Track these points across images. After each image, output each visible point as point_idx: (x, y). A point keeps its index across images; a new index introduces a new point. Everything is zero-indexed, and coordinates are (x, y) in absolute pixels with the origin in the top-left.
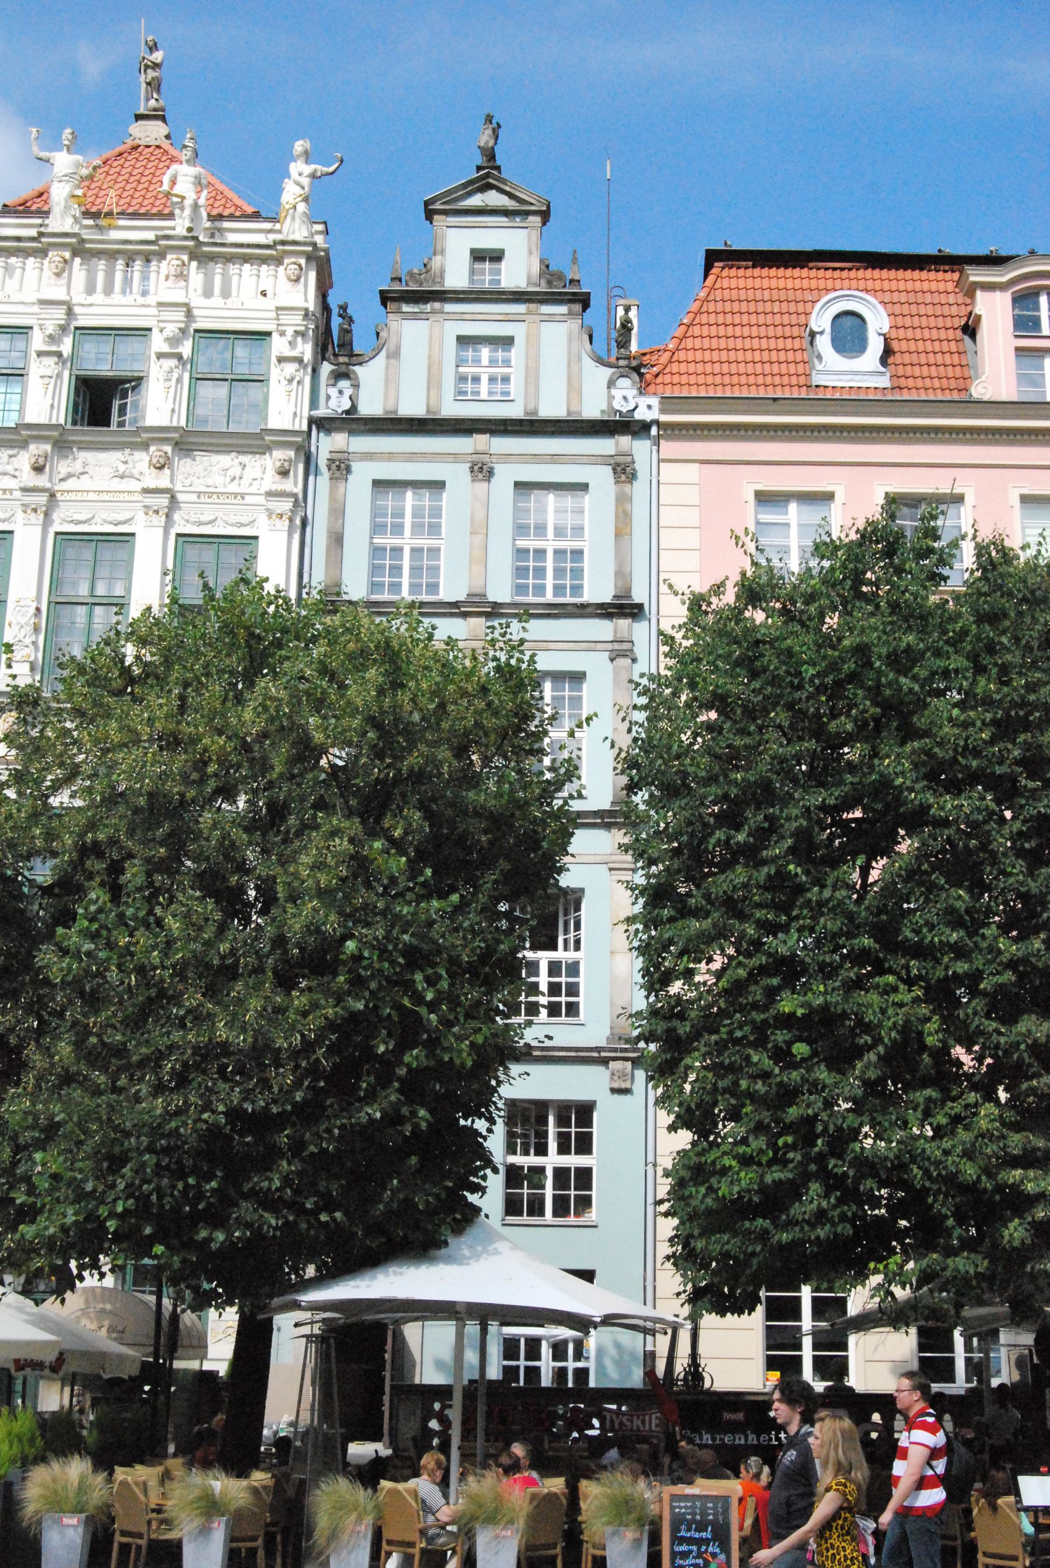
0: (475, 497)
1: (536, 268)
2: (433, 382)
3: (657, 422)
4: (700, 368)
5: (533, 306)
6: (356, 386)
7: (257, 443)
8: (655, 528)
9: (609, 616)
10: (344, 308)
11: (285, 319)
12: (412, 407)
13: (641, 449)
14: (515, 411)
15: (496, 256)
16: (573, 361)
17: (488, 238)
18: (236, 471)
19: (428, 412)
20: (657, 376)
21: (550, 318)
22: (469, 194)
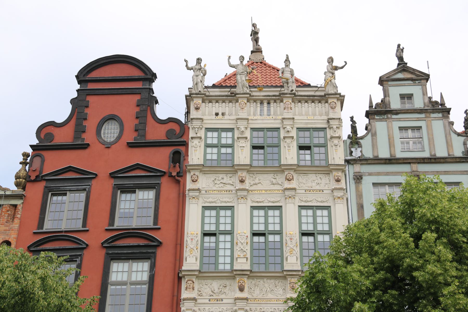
1: (427, 100)
2: (391, 144)
5: (428, 115)
7: (327, 169)
12: (384, 154)
14: (426, 155)
15: (410, 97)
21: (436, 119)
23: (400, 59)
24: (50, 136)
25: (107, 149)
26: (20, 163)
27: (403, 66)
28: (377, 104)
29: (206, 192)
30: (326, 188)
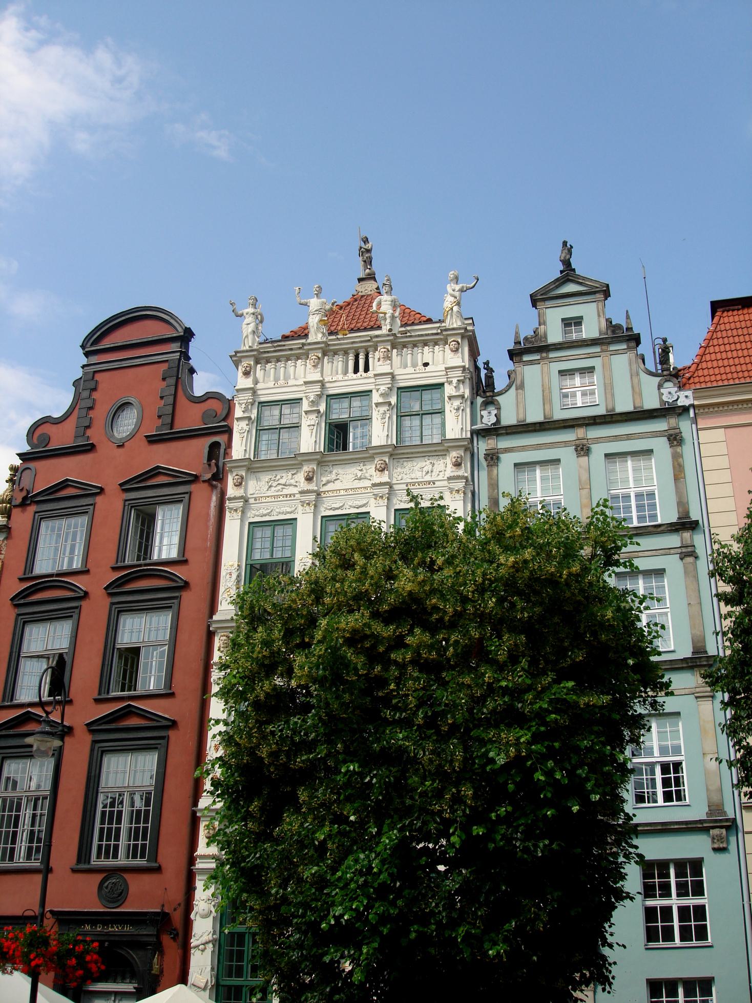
0: (580, 467)
1: (604, 324)
2: (546, 399)
3: (693, 406)
4: (717, 371)
5: (604, 347)
6: (499, 409)
7: (440, 449)
8: (701, 472)
9: (677, 531)
10: (487, 363)
11: (451, 374)
12: (535, 416)
13: (685, 426)
14: (601, 411)
15: (577, 321)
16: (634, 375)
17: (571, 311)
18: (429, 468)
19: (545, 418)
20: (689, 379)
21: (617, 352)
22: (557, 287)
23: (567, 263)
24: (46, 439)
25: (121, 450)
26: (7, 481)
27: (568, 274)
28: (526, 339)
29: (255, 500)
30: (440, 478)
